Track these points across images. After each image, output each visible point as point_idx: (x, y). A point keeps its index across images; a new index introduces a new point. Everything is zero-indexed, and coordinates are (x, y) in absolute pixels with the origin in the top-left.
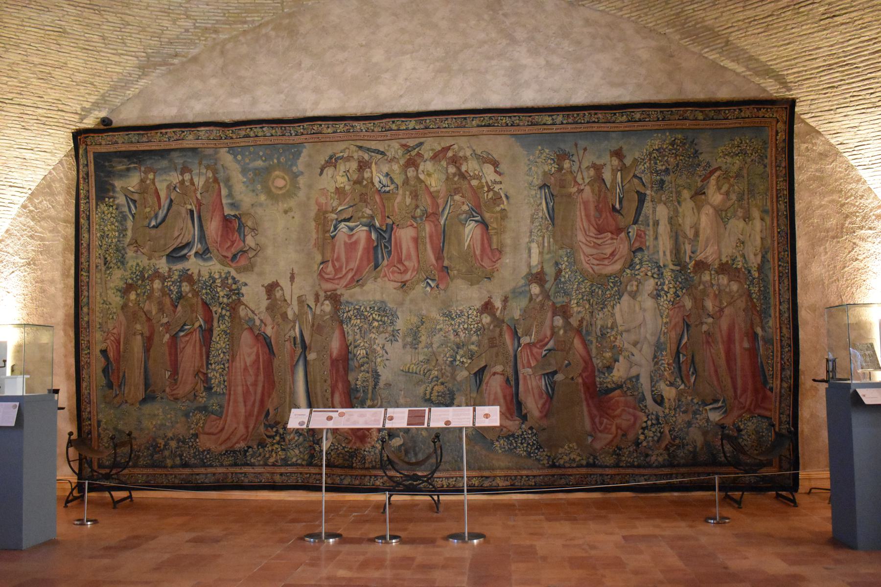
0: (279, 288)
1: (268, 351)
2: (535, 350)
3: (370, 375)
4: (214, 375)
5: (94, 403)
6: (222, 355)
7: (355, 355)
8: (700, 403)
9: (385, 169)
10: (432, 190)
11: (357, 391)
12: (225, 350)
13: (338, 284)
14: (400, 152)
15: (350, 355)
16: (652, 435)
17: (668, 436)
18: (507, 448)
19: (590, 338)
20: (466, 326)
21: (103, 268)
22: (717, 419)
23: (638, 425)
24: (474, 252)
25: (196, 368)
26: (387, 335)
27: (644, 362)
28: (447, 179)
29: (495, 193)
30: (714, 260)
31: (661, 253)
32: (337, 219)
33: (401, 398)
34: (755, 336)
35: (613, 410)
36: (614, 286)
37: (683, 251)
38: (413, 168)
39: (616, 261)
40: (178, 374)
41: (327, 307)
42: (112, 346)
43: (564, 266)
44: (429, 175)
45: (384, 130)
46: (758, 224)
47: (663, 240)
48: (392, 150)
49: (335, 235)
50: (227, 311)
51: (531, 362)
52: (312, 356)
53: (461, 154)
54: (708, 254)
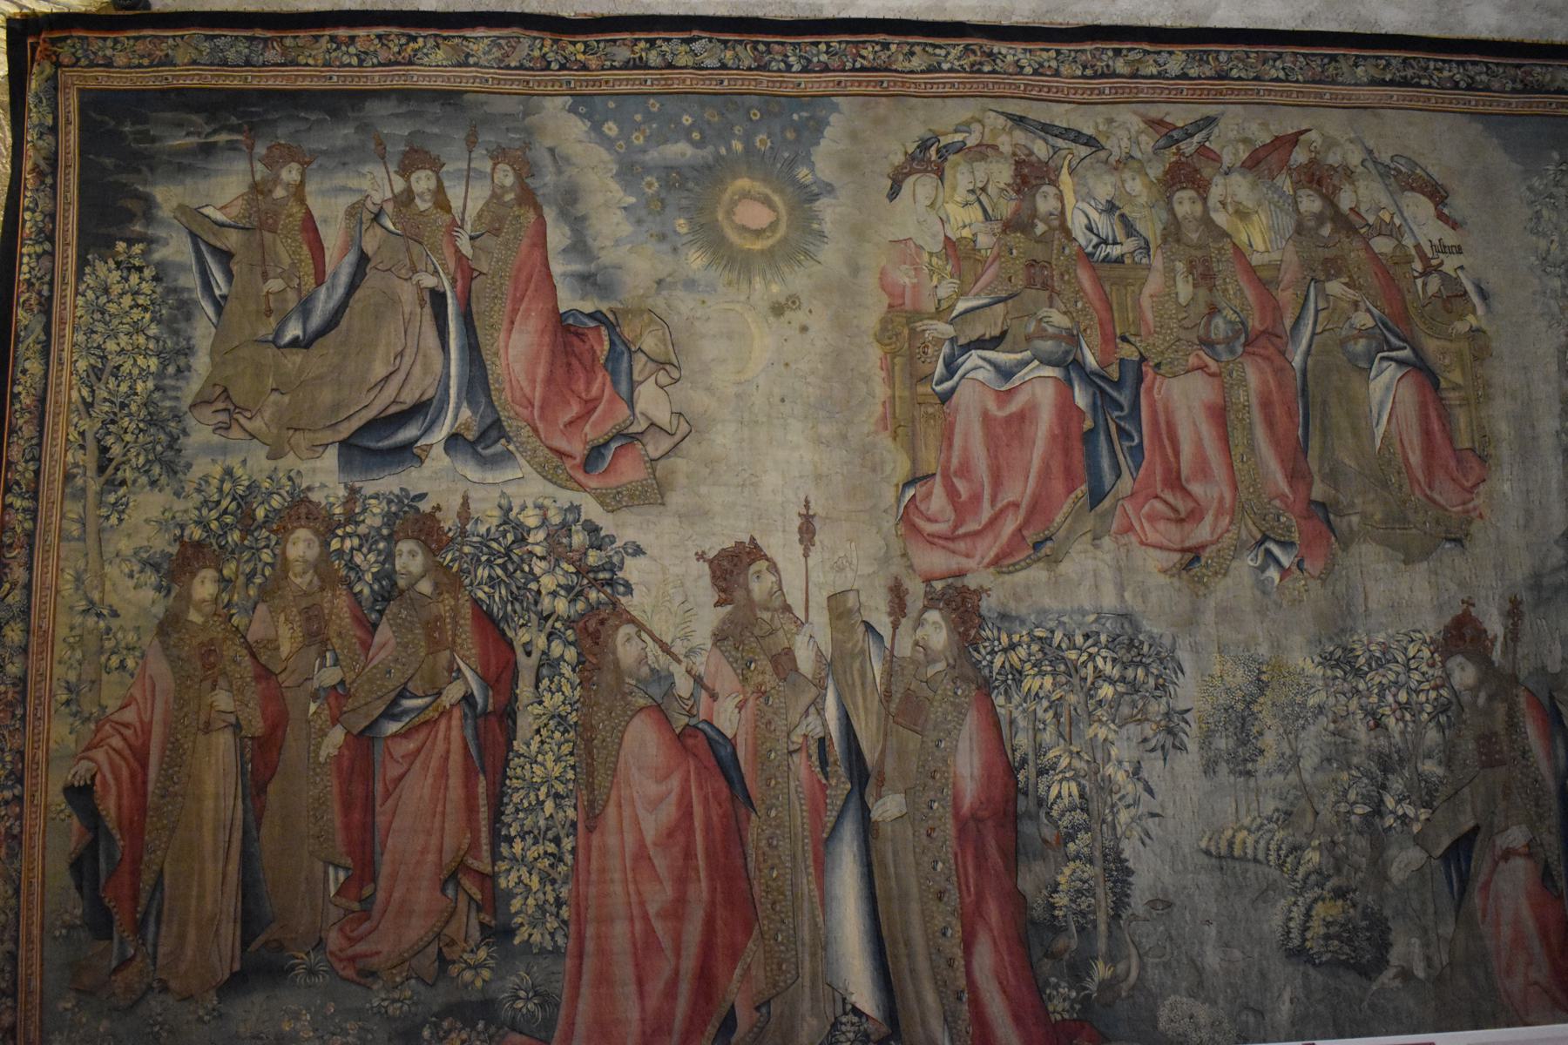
0: (762, 565)
1: (725, 793)
3: (1098, 870)
4: (520, 881)
5: (29, 993)
6: (549, 806)
7: (1040, 802)
9: (1104, 188)
10: (1255, 260)
11: (1054, 927)
12: (560, 788)
13: (967, 556)
14: (1147, 142)
15: (1022, 803)
20: (1403, 697)
21: (94, 486)
24: (1406, 460)
25: (447, 858)
26: (1148, 729)
28: (1300, 229)
29: (1445, 277)
32: (953, 340)
33: (1209, 950)
38: (1190, 193)
40: (374, 879)
41: (937, 632)
42: (117, 779)
44: (1242, 214)
45: (1089, 72)
48: (1122, 133)
49: (953, 390)
50: (567, 643)
52: (888, 807)
53: (1333, 159)
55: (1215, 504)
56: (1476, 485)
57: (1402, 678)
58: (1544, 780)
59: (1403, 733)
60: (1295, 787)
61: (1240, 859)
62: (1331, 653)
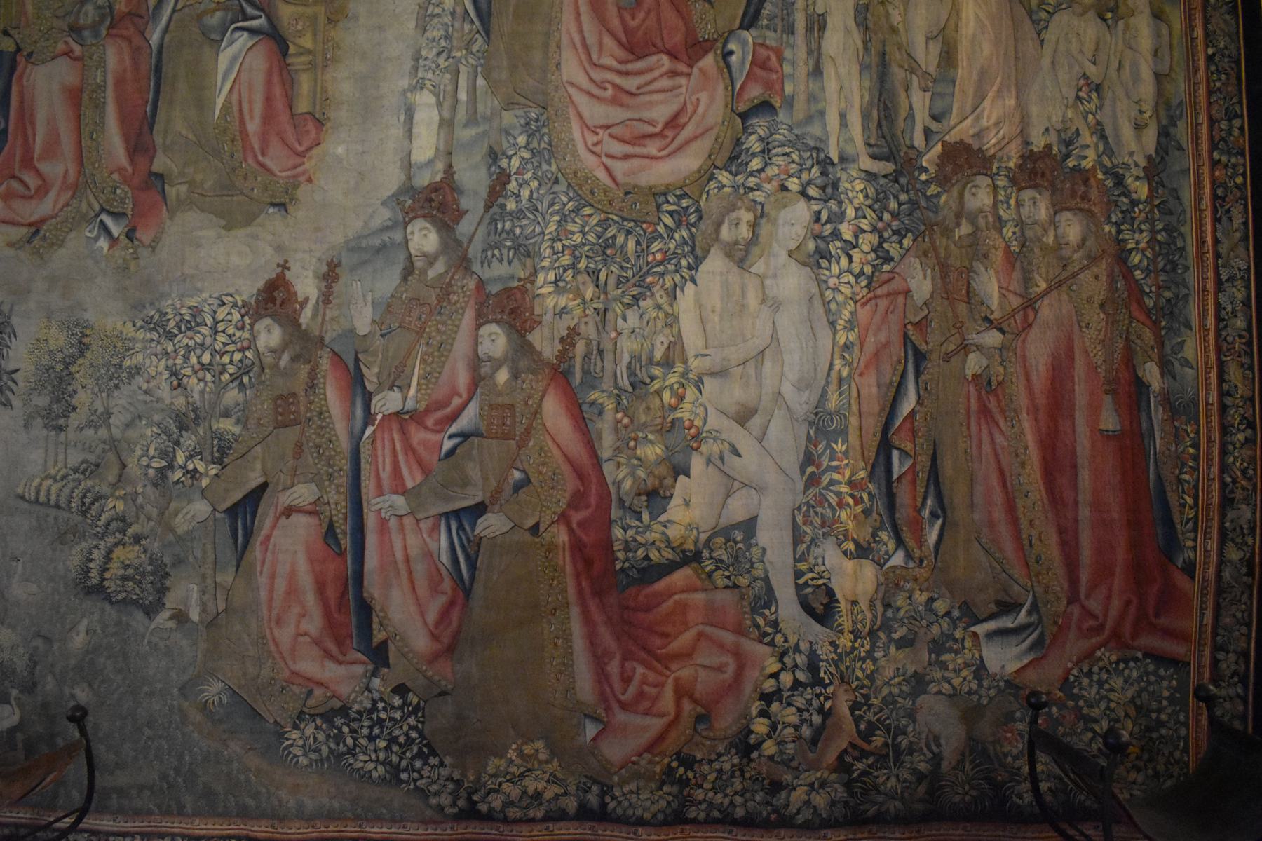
2: (418, 436)
8: (956, 613)
16: (794, 719)
17: (849, 725)
18: (325, 750)
19: (594, 395)
20: (206, 358)
22: (1012, 667)
23: (748, 688)
27: (771, 477)
30: (1003, 145)
31: (832, 120)
34: (1140, 387)
35: (665, 635)
36: (679, 225)
37: (903, 113)
39: (687, 142)
43: (515, 162)
46: (1143, 26)
47: (838, 76)
51: (405, 472)
54: (984, 123)
55: (59, 182)
56: (310, 149)
57: (208, 341)
58: (338, 440)
59: (202, 392)
60: (104, 442)
61: (41, 504)
62: (152, 317)
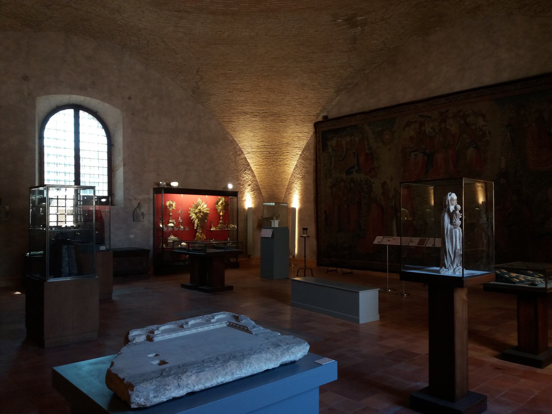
49: (409, 159)
